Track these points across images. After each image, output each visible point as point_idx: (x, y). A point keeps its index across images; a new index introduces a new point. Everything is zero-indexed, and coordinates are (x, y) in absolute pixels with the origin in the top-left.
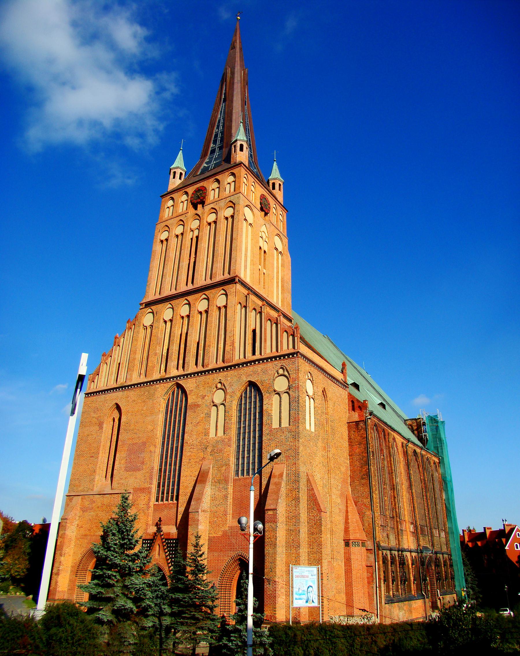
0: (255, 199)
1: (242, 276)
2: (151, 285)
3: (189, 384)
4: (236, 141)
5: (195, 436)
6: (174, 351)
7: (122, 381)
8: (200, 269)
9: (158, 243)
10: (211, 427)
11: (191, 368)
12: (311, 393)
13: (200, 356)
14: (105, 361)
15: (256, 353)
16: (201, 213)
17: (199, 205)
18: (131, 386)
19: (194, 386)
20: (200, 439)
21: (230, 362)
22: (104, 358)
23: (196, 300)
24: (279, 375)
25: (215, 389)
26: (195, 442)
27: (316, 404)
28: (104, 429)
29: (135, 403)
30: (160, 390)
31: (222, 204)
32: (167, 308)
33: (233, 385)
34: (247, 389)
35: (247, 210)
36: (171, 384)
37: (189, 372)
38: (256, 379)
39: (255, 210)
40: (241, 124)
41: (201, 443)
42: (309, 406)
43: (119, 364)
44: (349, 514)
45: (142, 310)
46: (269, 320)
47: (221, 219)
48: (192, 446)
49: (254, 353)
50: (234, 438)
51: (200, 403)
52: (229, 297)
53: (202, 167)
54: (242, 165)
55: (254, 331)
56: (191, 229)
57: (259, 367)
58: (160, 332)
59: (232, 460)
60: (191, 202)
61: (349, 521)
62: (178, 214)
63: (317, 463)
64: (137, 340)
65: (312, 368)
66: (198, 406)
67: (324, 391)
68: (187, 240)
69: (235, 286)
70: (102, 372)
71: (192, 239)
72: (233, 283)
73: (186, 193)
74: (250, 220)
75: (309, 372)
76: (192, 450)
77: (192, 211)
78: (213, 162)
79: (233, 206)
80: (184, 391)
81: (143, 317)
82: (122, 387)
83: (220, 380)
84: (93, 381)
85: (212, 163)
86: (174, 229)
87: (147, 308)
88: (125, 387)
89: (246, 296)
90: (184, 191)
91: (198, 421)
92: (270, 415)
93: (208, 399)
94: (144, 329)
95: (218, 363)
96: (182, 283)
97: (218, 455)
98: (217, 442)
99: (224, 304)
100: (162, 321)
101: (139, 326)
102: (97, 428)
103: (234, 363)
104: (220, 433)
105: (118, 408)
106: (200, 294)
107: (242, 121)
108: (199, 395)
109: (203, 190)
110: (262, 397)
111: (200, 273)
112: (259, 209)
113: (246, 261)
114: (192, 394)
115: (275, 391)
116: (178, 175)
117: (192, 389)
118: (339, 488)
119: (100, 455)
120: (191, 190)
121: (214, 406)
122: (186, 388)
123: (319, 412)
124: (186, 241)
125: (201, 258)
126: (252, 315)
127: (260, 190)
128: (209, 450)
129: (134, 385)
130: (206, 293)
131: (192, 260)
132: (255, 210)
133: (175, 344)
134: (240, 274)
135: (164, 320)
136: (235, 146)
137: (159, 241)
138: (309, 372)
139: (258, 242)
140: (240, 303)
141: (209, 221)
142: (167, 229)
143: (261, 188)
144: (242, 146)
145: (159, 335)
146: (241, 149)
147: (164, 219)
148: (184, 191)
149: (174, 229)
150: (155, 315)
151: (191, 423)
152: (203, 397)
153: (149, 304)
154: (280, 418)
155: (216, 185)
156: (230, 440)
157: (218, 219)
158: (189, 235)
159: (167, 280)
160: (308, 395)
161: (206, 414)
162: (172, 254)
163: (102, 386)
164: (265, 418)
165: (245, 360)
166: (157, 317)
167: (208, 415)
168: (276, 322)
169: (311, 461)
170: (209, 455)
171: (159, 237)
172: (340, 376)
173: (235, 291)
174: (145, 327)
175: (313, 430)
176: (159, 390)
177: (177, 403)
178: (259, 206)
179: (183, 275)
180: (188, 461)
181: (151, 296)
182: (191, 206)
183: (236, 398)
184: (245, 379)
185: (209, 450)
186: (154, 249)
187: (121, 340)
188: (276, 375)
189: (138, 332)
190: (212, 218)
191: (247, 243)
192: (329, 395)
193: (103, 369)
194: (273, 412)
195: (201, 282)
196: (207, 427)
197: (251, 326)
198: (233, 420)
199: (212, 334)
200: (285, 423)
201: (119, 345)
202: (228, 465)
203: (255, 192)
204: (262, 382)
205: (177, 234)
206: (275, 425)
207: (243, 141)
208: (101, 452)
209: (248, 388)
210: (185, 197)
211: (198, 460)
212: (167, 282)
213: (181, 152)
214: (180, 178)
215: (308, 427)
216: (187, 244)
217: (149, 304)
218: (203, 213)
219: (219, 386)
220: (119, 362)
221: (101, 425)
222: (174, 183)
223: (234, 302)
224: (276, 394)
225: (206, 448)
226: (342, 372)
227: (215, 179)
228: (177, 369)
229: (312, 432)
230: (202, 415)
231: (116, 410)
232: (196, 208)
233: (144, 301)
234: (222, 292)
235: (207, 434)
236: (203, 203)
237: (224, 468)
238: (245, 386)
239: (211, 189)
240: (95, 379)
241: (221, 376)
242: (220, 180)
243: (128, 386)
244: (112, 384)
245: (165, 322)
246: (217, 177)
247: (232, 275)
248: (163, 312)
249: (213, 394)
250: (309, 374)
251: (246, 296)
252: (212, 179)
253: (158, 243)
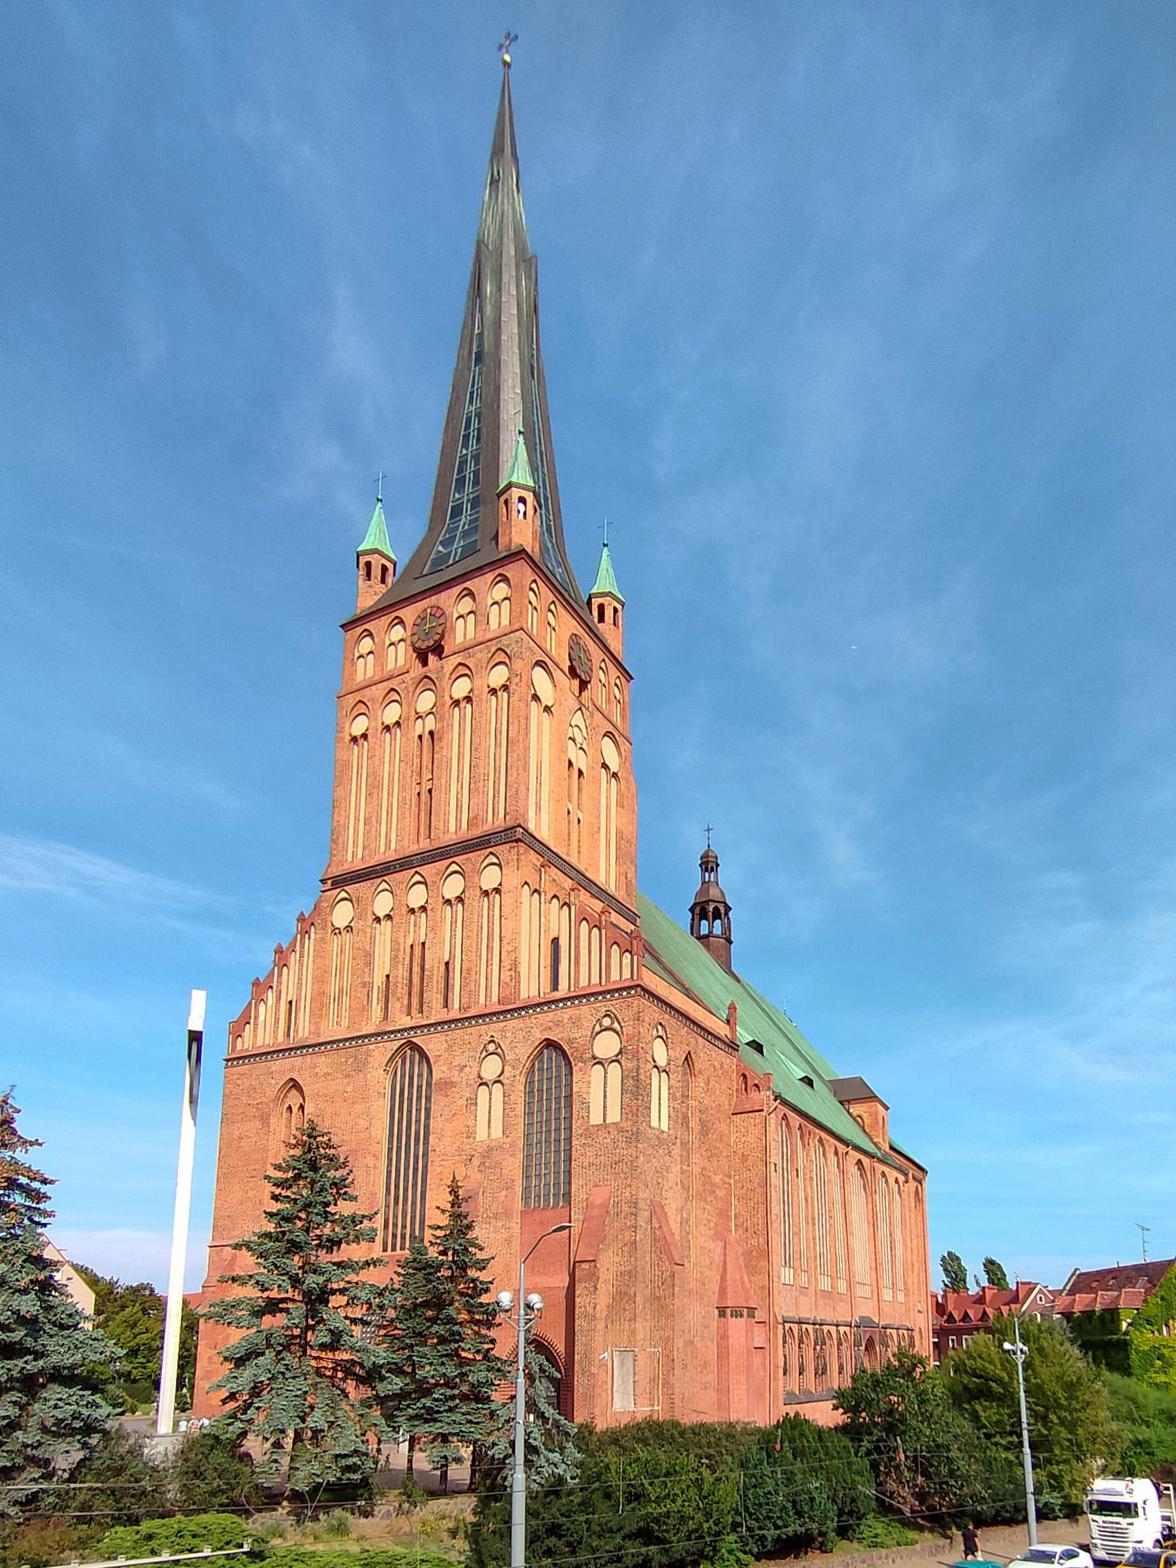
0: (558, 645)
1: (531, 827)
3: (432, 1044)
4: (510, 486)
6: (400, 980)
8: (443, 809)
11: (437, 1013)
12: (662, 1062)
20: (458, 1144)
27: (672, 1082)
30: (377, 1055)
35: (539, 674)
36: (397, 1044)
38: (560, 1036)
39: (557, 674)
40: (521, 439)
41: (460, 1150)
42: (660, 1089)
44: (728, 1266)
47: (481, 693)
49: (555, 987)
55: (555, 941)
57: (565, 1014)
58: (368, 940)
61: (728, 1277)
63: (670, 1184)
65: (666, 1016)
66: (453, 1084)
67: (688, 1058)
71: (420, 737)
74: (548, 700)
75: (660, 1024)
77: (418, 670)
78: (458, 544)
79: (507, 661)
80: (423, 1055)
83: (492, 1036)
85: (455, 547)
87: (338, 890)
92: (586, 1105)
93: (470, 1073)
98: (490, 1149)
107: (522, 430)
110: (571, 1068)
111: (442, 815)
112: (567, 671)
113: (539, 792)
114: (439, 1063)
115: (594, 1057)
117: (439, 1053)
118: (712, 1225)
123: (678, 1095)
127: (568, 625)
132: (557, 674)
133: (400, 966)
134: (526, 821)
136: (506, 502)
138: (660, 1024)
139: (564, 751)
141: (456, 696)
143: (570, 618)
154: (605, 1107)
157: (476, 692)
160: (656, 1067)
169: (660, 1180)
172: (723, 1030)
175: (664, 1127)
176: (375, 1053)
177: (411, 1078)
178: (566, 665)
184: (539, 1036)
190: (461, 688)
191: (540, 751)
192: (698, 1065)
199: (474, 946)
200: (614, 1116)
203: (557, 628)
204: (570, 1042)
206: (596, 1118)
207: (525, 488)
212: (373, 833)
214: (383, 581)
215: (654, 1124)
226: (728, 1022)
227: (465, 589)
228: (409, 1014)
229: (663, 1132)
232: (425, 663)
236: (438, 650)
246: (467, 584)
250: (660, 1028)
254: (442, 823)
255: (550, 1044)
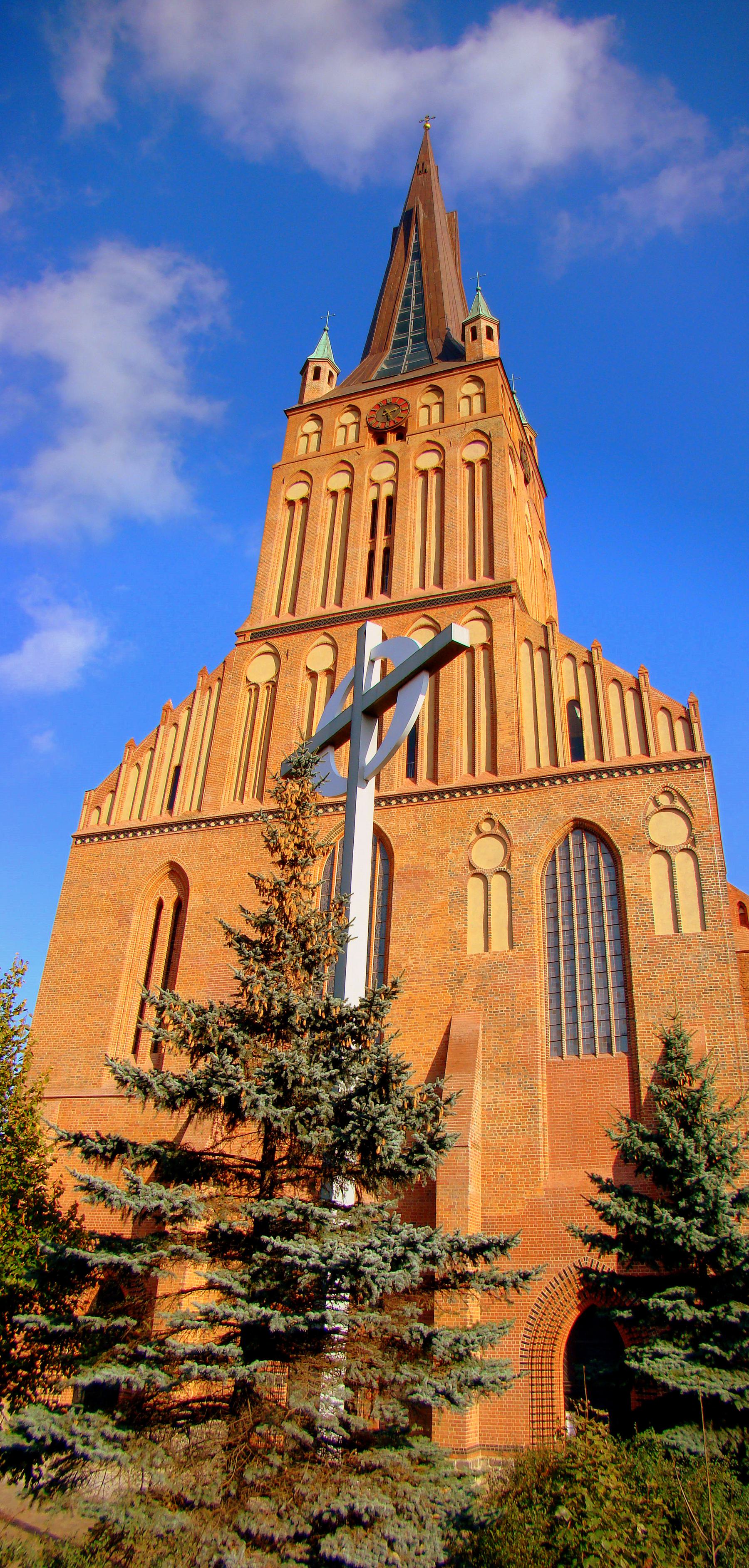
2: (267, 593)
5: (422, 950)
7: (184, 807)
9: (281, 507)
10: (469, 929)
13: (422, 757)
14: (134, 760)
15: (586, 756)
16: (399, 449)
17: (389, 434)
18: (217, 820)
19: (411, 826)
21: (513, 773)
22: (132, 753)
23: (403, 627)
24: (661, 807)
25: (474, 836)
26: (422, 964)
28: (133, 926)
29: (230, 862)
31: (456, 433)
32: (315, 643)
33: (527, 828)
34: (567, 837)
37: (394, 792)
43: (178, 769)
45: (242, 647)
46: (614, 680)
48: (416, 976)
50: (542, 958)
51: (432, 867)
52: (496, 626)
53: (379, 369)
54: (499, 363)
56: (371, 480)
59: (542, 1014)
60: (369, 426)
62: (333, 450)
64: (231, 716)
68: (364, 502)
69: (510, 603)
70: (125, 786)
72: (505, 597)
73: (355, 410)
76: (414, 984)
81: (246, 663)
82: (189, 823)
84: (98, 808)
86: (325, 481)
88: (198, 822)
89: (545, 628)
90: (347, 404)
91: (429, 912)
92: (646, 905)
94: (250, 690)
95: (477, 773)
96: (357, 592)
97: (497, 998)
98: (493, 966)
99: (484, 639)
100: (303, 673)
101: (236, 683)
102: (112, 921)
103: (524, 775)
104: (499, 942)
105: (177, 873)
106: (416, 615)
108: (429, 847)
109: (402, 404)
116: (324, 375)
119: (122, 991)
120: (366, 404)
121: (474, 875)
122: (385, 831)
124: (360, 503)
125: (408, 539)
126: (564, 670)
128: (469, 985)
129: (226, 819)
130: (431, 613)
131: (381, 545)
135: (307, 668)
137: (282, 501)
140: (526, 640)
142: (304, 477)
144: (489, 331)
145: (297, 704)
146: (490, 336)
147: (295, 457)
148: (347, 404)
149: (325, 481)
150: (283, 659)
151: (409, 917)
152: (442, 854)
153: (260, 635)
155: (432, 398)
156: (530, 959)
158: (366, 496)
159: (312, 583)
161: (451, 896)
162: (320, 530)
163: (124, 818)
164: (632, 912)
165: (555, 771)
166: (289, 663)
167: (461, 899)
168: (634, 687)
170: (470, 998)
171: (283, 493)
173: (510, 613)
174: (253, 687)
179: (358, 575)
180: (404, 1012)
181: (266, 618)
182: (370, 435)
183: (539, 857)
185: (469, 985)
186: (270, 517)
187: (182, 714)
188: (652, 807)
189: (234, 697)
193: (127, 778)
194: (653, 895)
195: (409, 592)
196: (457, 927)
197: (565, 692)
198: (535, 911)
201: (176, 725)
202: (530, 1025)
204: (611, 822)
205: (333, 489)
208: (122, 985)
209: (570, 836)
210: (349, 418)
211: (434, 1011)
213: (325, 335)
216: (364, 510)
217: (260, 635)
218: (406, 451)
219: (486, 827)
220: (176, 762)
221: (123, 916)
222: (318, 389)
223: (512, 638)
224: (656, 852)
225: (460, 982)
230: (441, 898)
231: (167, 881)
233: (248, 627)
234: (476, 614)
235: (459, 943)
237: (519, 1032)
238: (562, 831)
239: (419, 404)
240: (103, 801)
241: (491, 803)
242: (443, 389)
243: (207, 821)
244: (156, 813)
245: (313, 675)
247: (499, 578)
248: (305, 654)
249: (470, 847)
251: (545, 628)
252: (424, 386)
253: (281, 507)
254: (406, 578)
255: (581, 826)
